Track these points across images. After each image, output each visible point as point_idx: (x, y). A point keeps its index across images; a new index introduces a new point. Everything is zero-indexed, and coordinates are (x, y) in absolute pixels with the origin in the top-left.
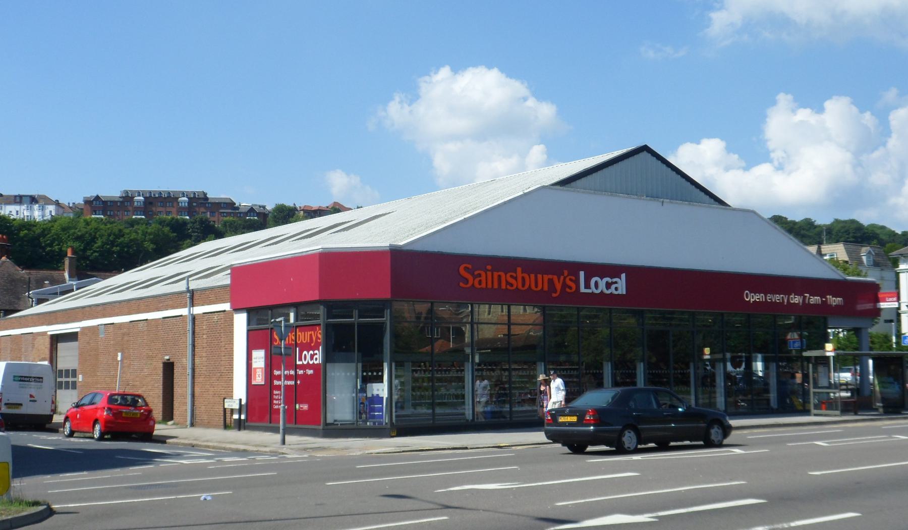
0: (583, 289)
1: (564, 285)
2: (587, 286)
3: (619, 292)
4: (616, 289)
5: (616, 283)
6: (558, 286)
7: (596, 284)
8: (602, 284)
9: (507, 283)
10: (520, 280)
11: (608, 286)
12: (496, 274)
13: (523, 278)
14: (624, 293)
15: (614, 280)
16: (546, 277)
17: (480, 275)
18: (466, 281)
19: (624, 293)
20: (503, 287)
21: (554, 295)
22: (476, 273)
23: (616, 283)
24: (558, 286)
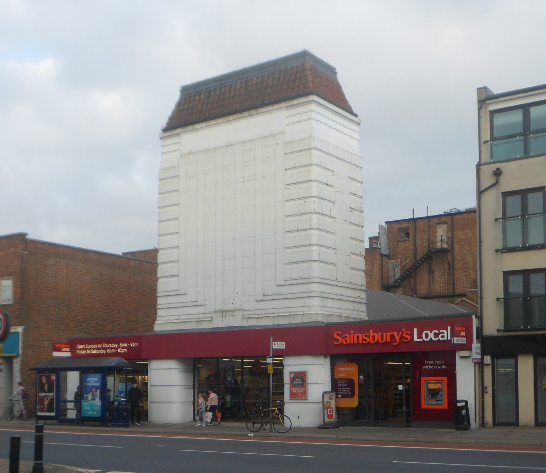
0: (416, 339)
1: (402, 337)
2: (420, 336)
3: (445, 338)
4: (443, 337)
5: (443, 333)
6: (397, 338)
7: (427, 335)
9: (363, 340)
11: (436, 335)
12: (356, 335)
13: (374, 336)
15: (441, 331)
16: (389, 334)
17: (346, 337)
18: (338, 340)
20: (361, 341)
21: (395, 344)
22: (344, 336)
23: (443, 333)
24: (397, 338)
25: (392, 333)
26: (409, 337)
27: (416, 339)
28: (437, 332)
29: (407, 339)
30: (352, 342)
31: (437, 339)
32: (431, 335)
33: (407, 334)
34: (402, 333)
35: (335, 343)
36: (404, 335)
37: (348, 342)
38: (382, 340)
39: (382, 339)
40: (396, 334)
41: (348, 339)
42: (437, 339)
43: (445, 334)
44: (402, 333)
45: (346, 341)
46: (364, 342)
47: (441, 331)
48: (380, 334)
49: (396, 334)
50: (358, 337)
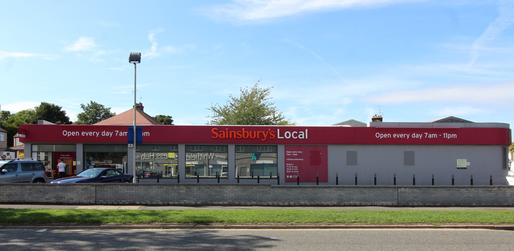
0: (279, 137)
6: (265, 136)
7: (288, 135)
9: (237, 135)
17: (222, 133)
20: (235, 137)
24: (265, 136)
25: (261, 132)
26: (274, 135)
28: (296, 133)
31: (296, 137)
34: (269, 132)
37: (224, 137)
38: (253, 136)
39: (253, 136)
40: (263, 132)
41: (224, 134)
42: (296, 137)
43: (303, 135)
44: (269, 132)
45: (222, 136)
48: (251, 132)
49: (263, 132)
50: (233, 133)
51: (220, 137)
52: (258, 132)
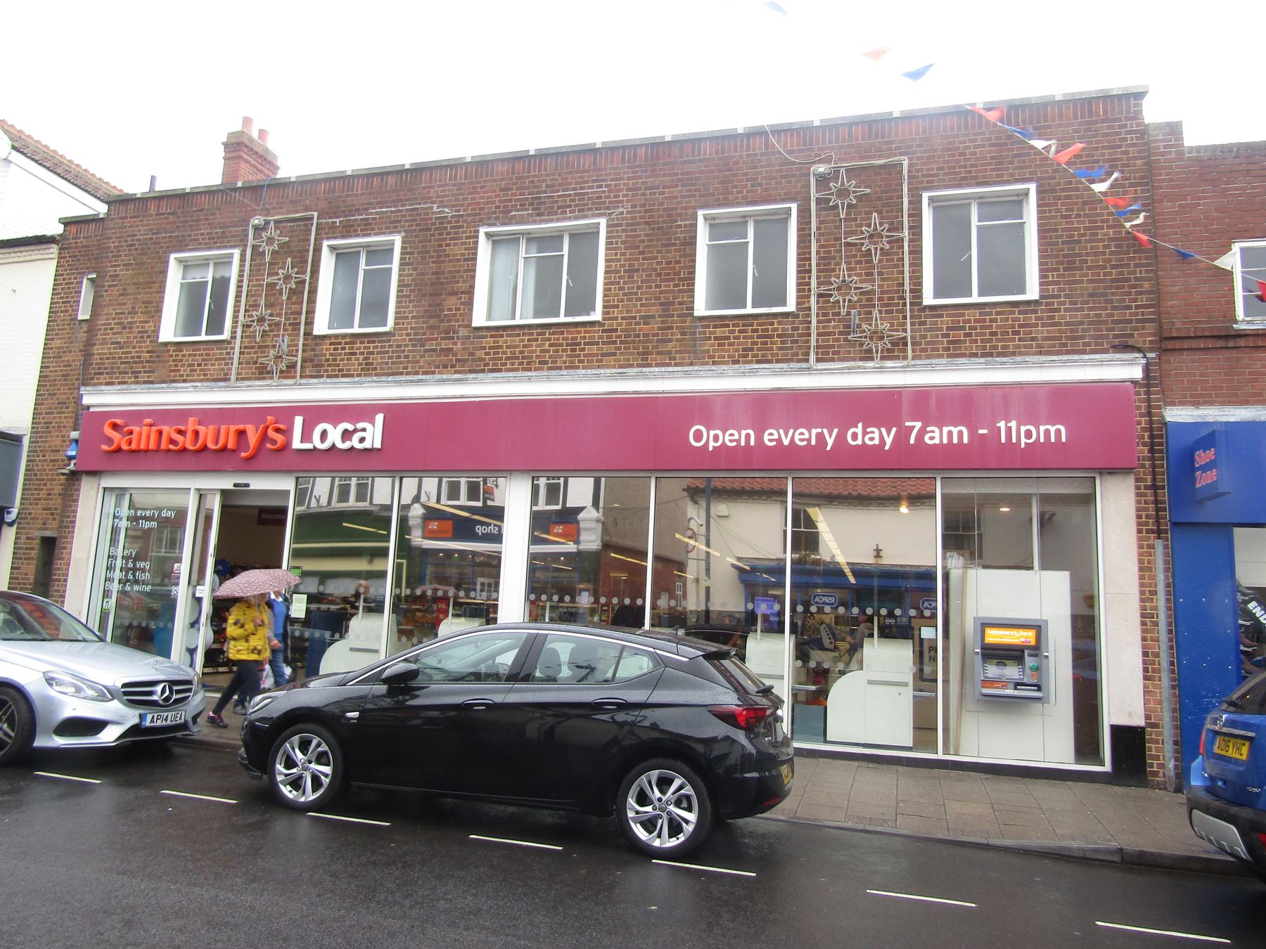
0: (297, 444)
1: (264, 437)
2: (306, 437)
3: (367, 445)
4: (362, 440)
5: (364, 430)
6: (252, 438)
7: (324, 435)
8: (335, 436)
10: (189, 435)
11: (346, 435)
13: (196, 433)
14: (378, 445)
15: (360, 426)
17: (131, 433)
18: (110, 441)
19: (378, 445)
20: (163, 446)
21: (243, 455)
23: (364, 430)
24: (252, 438)
25: (241, 427)
26: (280, 438)
27: (297, 444)
28: (350, 427)
29: (274, 442)
30: (142, 446)
32: (335, 436)
33: (278, 430)
35: (105, 447)
36: (271, 433)
37: (133, 446)
41: (134, 437)
44: (267, 428)
46: (171, 447)
47: (360, 426)
50: (160, 433)
51: (125, 447)
52: (233, 428)
